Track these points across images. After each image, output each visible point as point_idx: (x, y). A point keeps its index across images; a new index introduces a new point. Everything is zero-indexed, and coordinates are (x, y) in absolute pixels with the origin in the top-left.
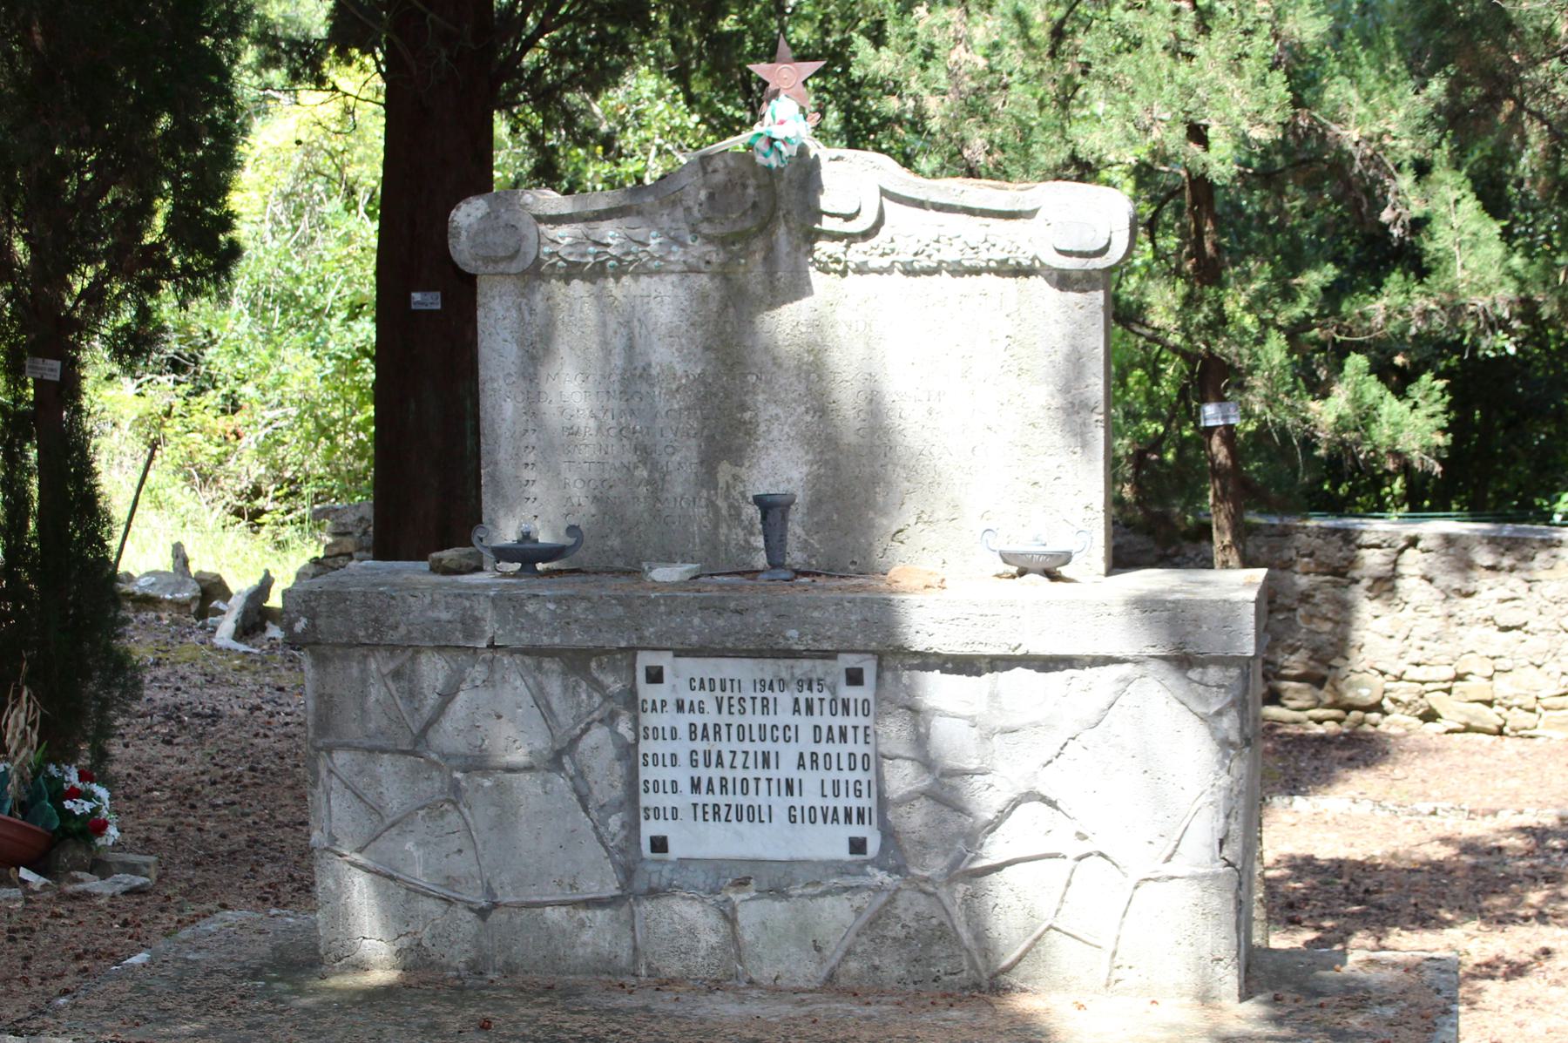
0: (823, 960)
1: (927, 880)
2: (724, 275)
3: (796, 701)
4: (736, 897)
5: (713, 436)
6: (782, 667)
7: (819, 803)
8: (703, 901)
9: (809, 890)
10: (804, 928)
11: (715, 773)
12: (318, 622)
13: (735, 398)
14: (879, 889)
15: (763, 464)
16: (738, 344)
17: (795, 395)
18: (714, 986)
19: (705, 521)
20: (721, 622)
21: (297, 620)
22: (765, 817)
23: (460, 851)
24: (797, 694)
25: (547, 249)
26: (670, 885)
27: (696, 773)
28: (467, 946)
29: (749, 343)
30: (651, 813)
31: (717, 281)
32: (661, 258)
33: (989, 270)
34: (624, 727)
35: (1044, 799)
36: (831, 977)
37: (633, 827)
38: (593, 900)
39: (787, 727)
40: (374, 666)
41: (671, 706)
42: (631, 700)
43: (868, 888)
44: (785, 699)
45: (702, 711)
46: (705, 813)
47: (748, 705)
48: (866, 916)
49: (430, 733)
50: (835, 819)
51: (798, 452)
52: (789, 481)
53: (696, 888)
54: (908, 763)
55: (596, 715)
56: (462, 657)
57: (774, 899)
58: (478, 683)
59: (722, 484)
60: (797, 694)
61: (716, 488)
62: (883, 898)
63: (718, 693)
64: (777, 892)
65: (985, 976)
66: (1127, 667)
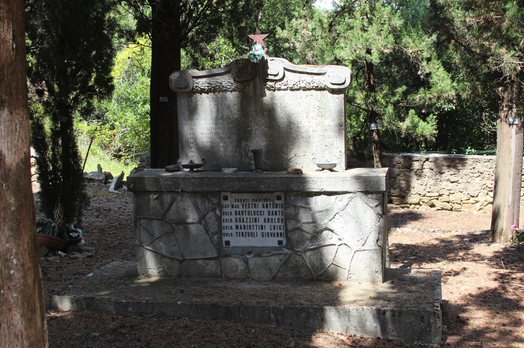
0: (271, 273)
1: (299, 251)
3: (263, 204)
4: (248, 257)
6: (260, 196)
7: (270, 231)
8: (239, 258)
9: (268, 254)
11: (242, 224)
14: (286, 254)
18: (243, 280)
22: (255, 235)
26: (231, 253)
27: (237, 224)
33: (313, 89)
34: (218, 212)
36: (274, 278)
37: (220, 239)
39: (261, 211)
41: (230, 206)
43: (283, 254)
44: (260, 204)
45: (238, 207)
47: (251, 206)
50: (274, 236)
51: (263, 138)
52: (261, 146)
55: (210, 209)
59: (243, 147)
62: (287, 257)
63: (243, 202)
64: (259, 255)
66: (352, 194)
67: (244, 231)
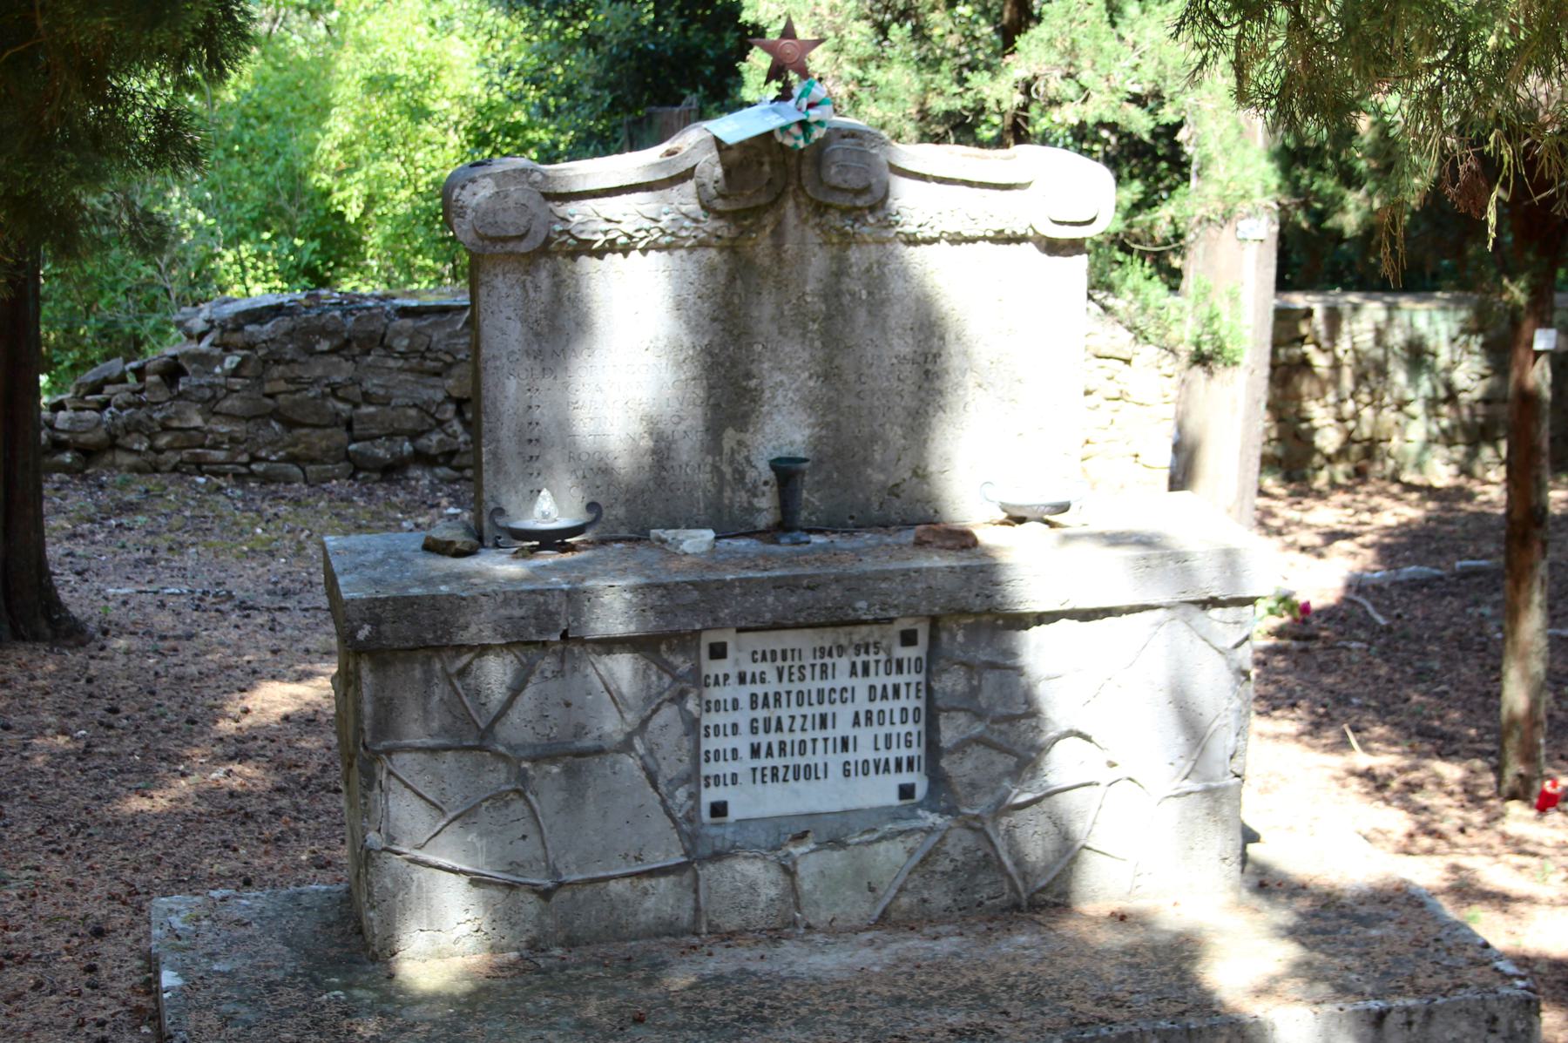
0: (876, 900)
1: (977, 817)
2: (732, 249)
3: (854, 665)
4: (797, 851)
5: (718, 405)
6: (842, 636)
7: (871, 756)
8: (764, 858)
9: (866, 837)
10: (860, 872)
11: (774, 738)
12: (383, 628)
13: (741, 367)
14: (930, 831)
15: (767, 429)
16: (745, 315)
17: (799, 362)
18: (776, 935)
19: (709, 486)
20: (793, 599)
21: (361, 627)
22: (821, 774)
23: (524, 837)
24: (854, 658)
25: (558, 228)
26: (733, 847)
27: (755, 740)
28: (528, 926)
29: (756, 314)
30: (712, 781)
31: (725, 254)
32: (673, 234)
33: (984, 238)
34: (691, 705)
35: (1079, 735)
36: (884, 915)
37: (694, 796)
38: (658, 869)
39: (844, 689)
40: (438, 666)
41: (733, 679)
42: (698, 680)
43: (921, 830)
44: (843, 663)
45: (763, 681)
46: (763, 775)
47: (808, 672)
48: (918, 856)
49: (497, 727)
50: (887, 769)
51: (801, 416)
52: (792, 443)
53: (758, 847)
54: (961, 714)
55: (667, 695)
56: (533, 651)
57: (832, 849)
58: (548, 674)
59: (726, 448)
60: (854, 658)
61: (721, 454)
62: (935, 838)
63: (779, 663)
64: (836, 843)
65: (1024, 896)
66: (1160, 612)
67: (778, 761)
